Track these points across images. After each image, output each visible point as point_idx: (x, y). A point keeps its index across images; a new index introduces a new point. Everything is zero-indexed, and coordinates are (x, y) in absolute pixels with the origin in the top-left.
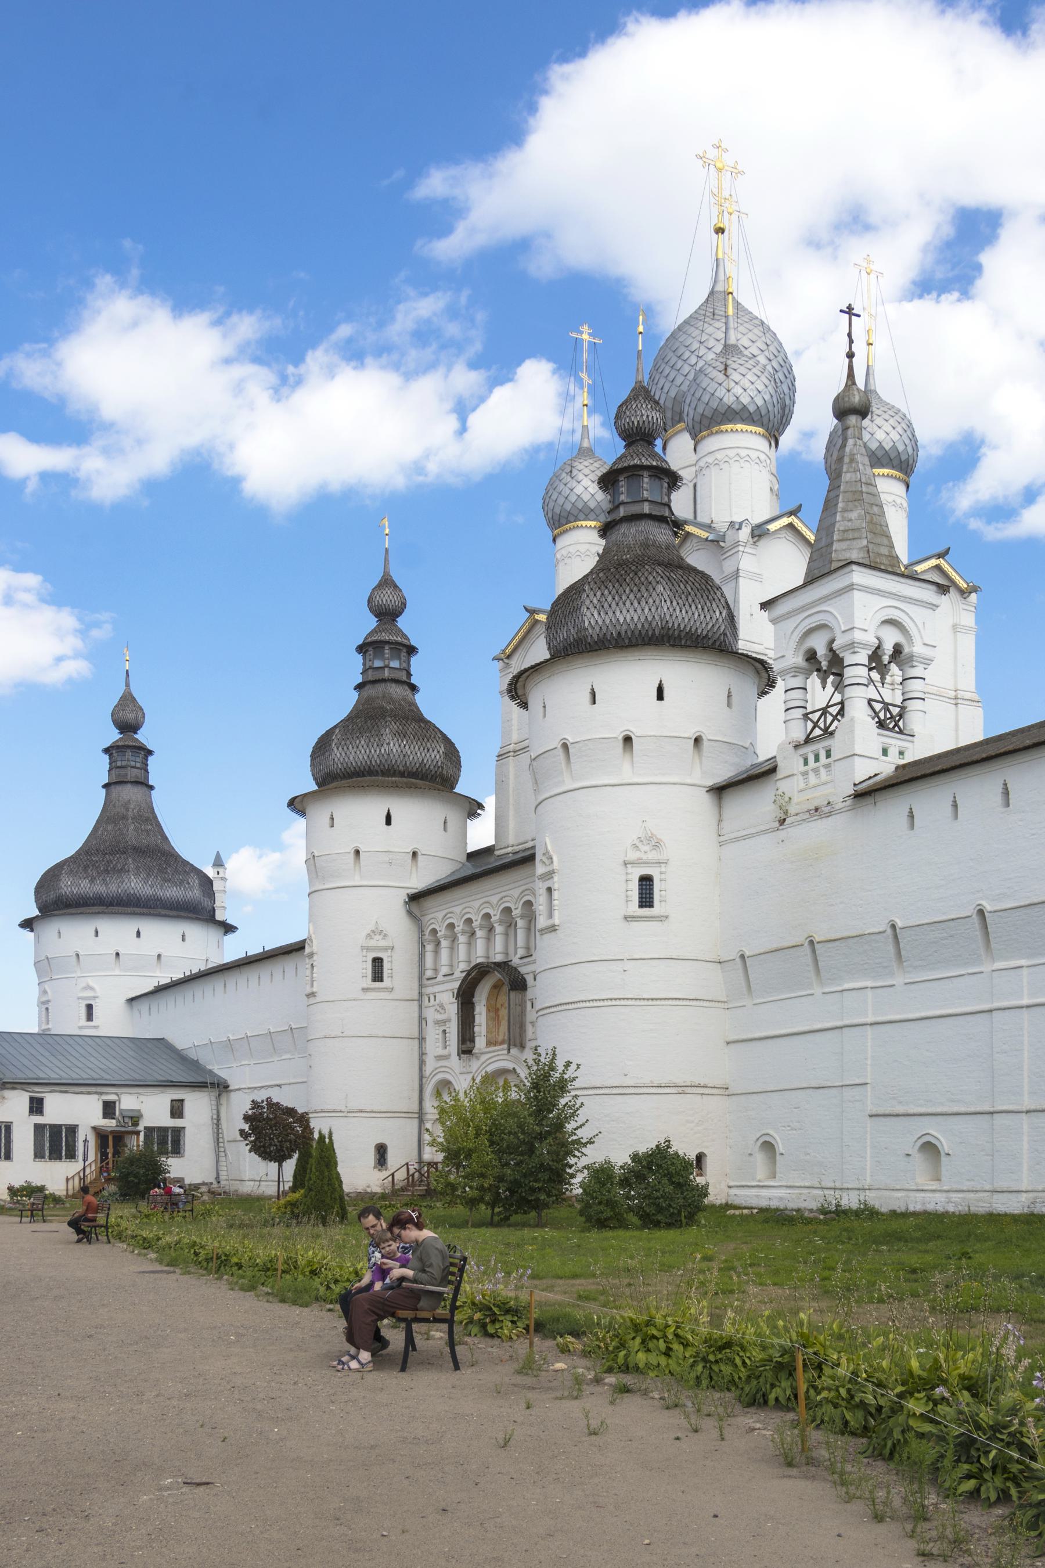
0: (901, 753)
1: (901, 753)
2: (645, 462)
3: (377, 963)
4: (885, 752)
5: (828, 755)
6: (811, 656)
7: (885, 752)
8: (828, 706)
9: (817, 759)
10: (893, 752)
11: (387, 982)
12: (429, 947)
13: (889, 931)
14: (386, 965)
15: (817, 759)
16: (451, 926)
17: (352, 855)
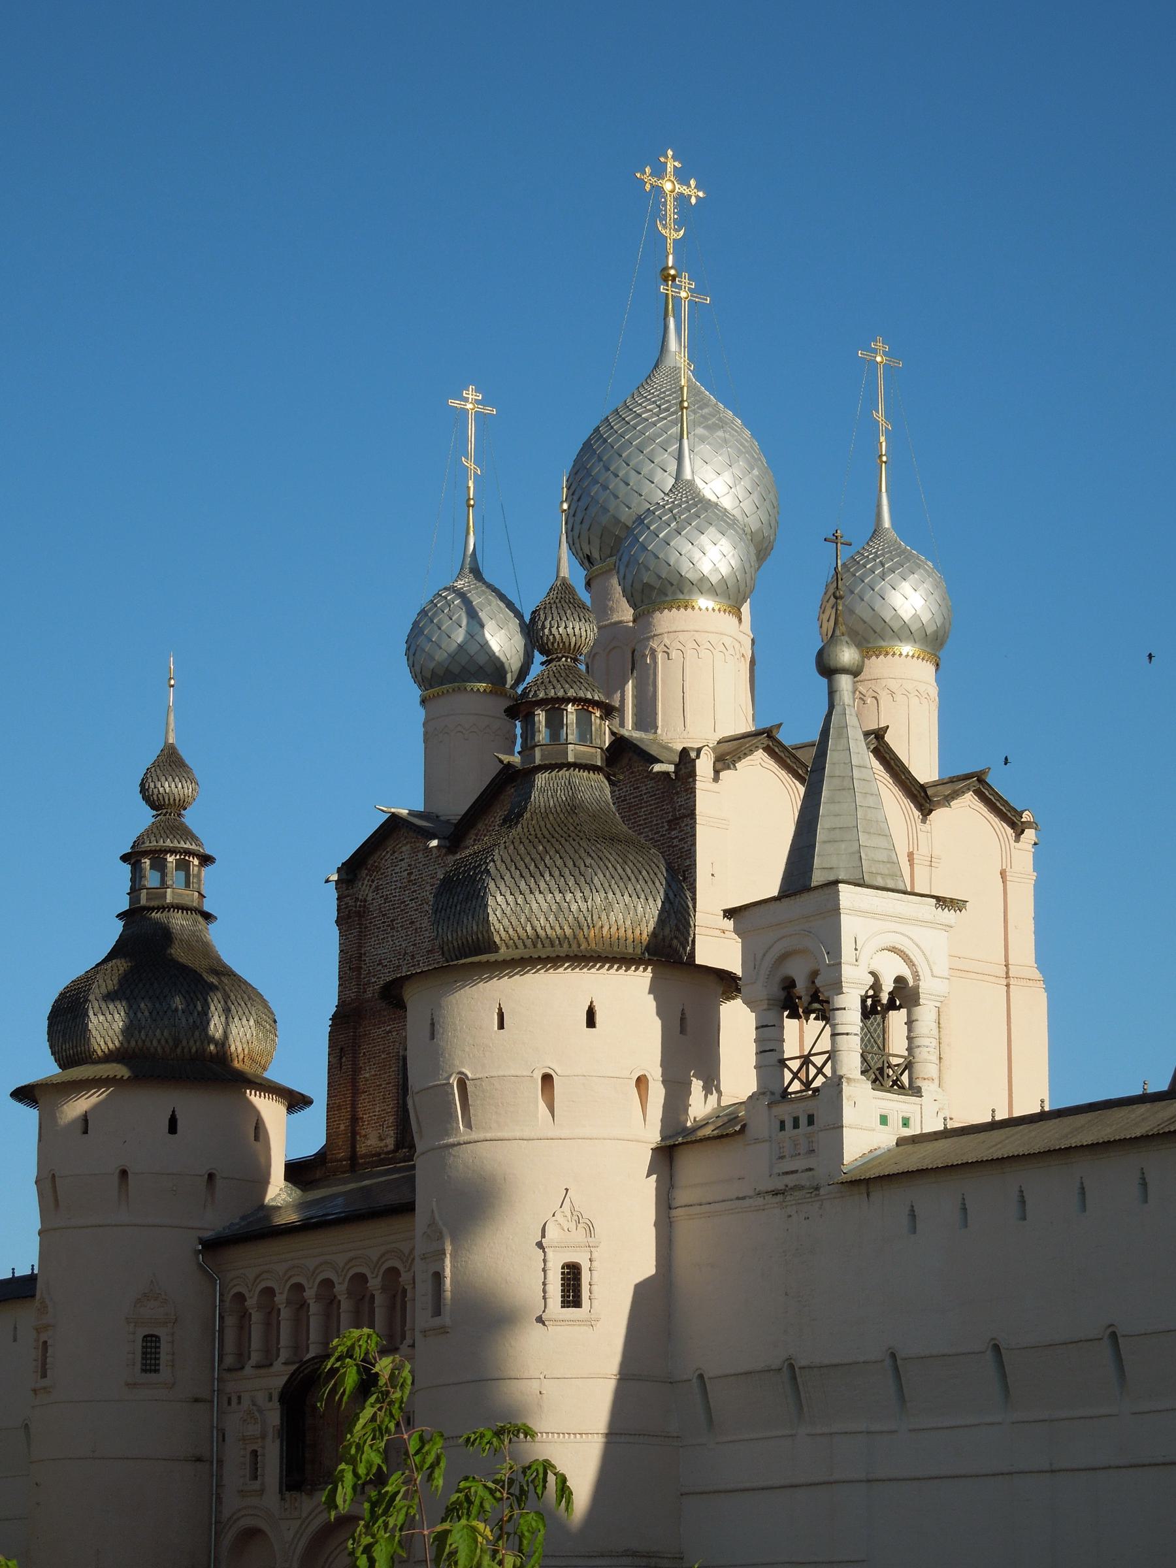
0: (906, 1123)
1: (906, 1123)
2: (571, 693)
3: (151, 1343)
4: (884, 1120)
5: (811, 1120)
6: (789, 985)
7: (884, 1120)
8: (810, 1054)
9: (796, 1125)
10: (895, 1120)
11: (165, 1372)
12: (230, 1321)
13: (888, 1362)
14: (164, 1347)
15: (796, 1125)
16: (269, 1292)
17: (115, 1179)
